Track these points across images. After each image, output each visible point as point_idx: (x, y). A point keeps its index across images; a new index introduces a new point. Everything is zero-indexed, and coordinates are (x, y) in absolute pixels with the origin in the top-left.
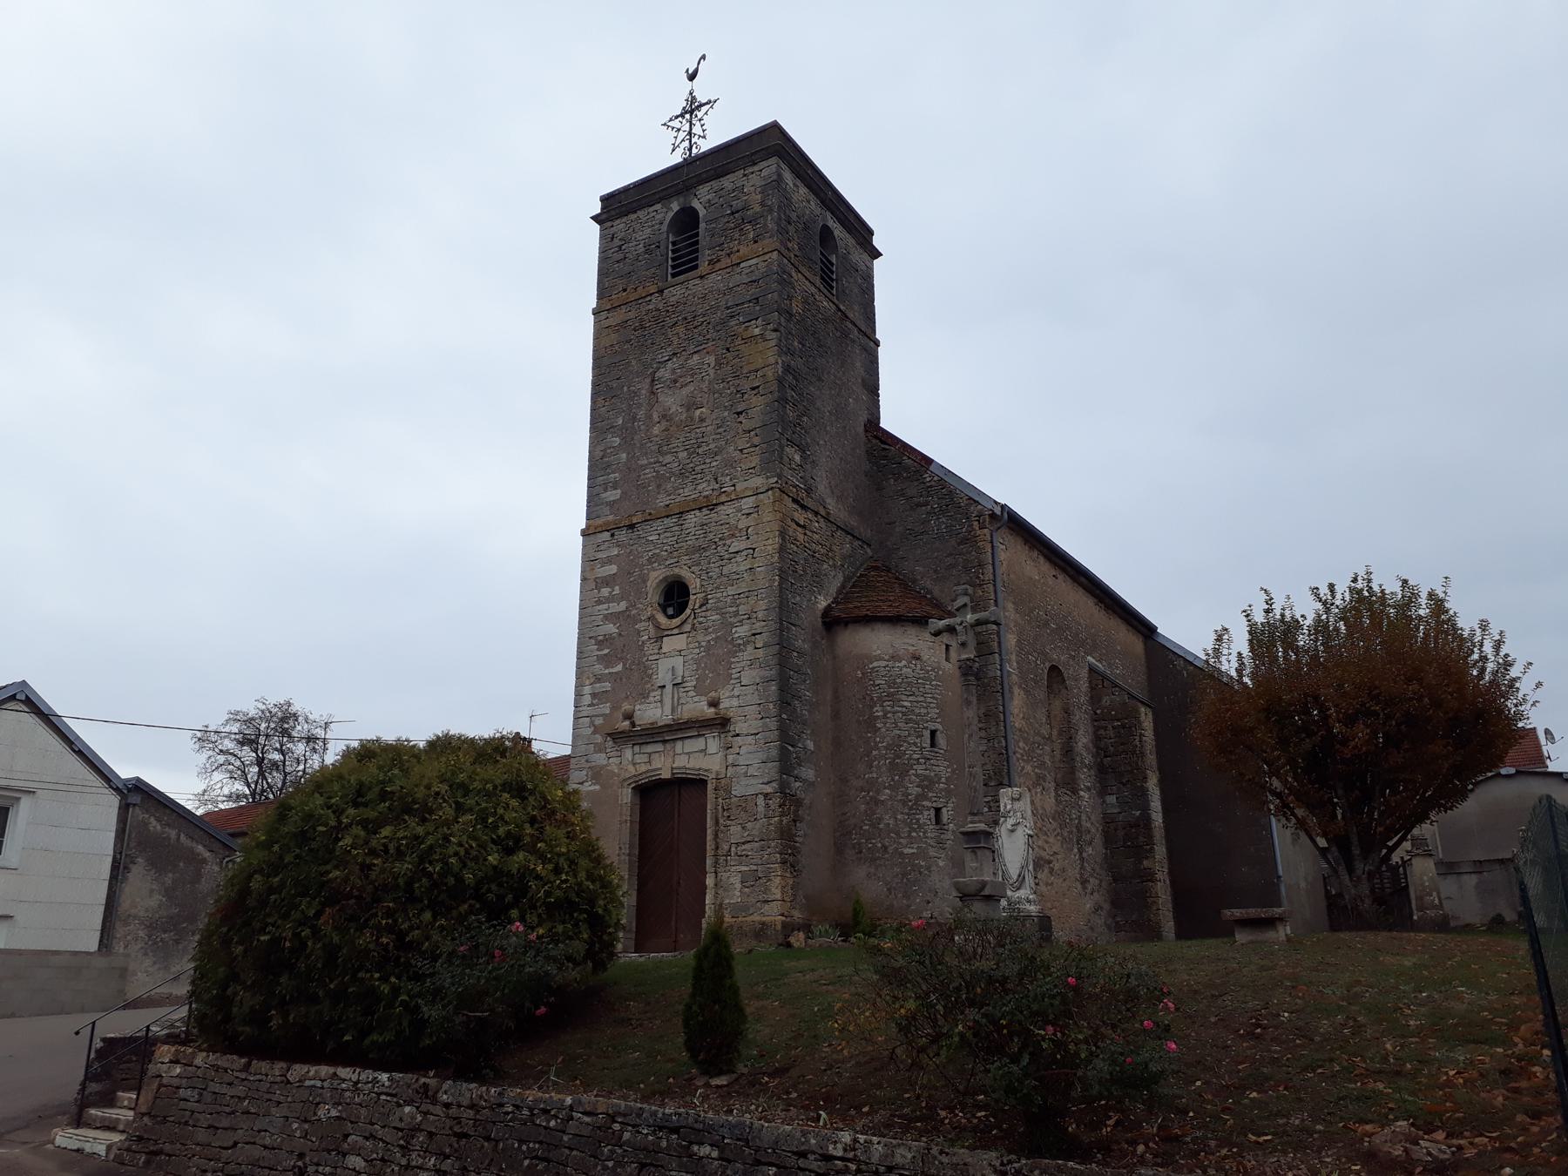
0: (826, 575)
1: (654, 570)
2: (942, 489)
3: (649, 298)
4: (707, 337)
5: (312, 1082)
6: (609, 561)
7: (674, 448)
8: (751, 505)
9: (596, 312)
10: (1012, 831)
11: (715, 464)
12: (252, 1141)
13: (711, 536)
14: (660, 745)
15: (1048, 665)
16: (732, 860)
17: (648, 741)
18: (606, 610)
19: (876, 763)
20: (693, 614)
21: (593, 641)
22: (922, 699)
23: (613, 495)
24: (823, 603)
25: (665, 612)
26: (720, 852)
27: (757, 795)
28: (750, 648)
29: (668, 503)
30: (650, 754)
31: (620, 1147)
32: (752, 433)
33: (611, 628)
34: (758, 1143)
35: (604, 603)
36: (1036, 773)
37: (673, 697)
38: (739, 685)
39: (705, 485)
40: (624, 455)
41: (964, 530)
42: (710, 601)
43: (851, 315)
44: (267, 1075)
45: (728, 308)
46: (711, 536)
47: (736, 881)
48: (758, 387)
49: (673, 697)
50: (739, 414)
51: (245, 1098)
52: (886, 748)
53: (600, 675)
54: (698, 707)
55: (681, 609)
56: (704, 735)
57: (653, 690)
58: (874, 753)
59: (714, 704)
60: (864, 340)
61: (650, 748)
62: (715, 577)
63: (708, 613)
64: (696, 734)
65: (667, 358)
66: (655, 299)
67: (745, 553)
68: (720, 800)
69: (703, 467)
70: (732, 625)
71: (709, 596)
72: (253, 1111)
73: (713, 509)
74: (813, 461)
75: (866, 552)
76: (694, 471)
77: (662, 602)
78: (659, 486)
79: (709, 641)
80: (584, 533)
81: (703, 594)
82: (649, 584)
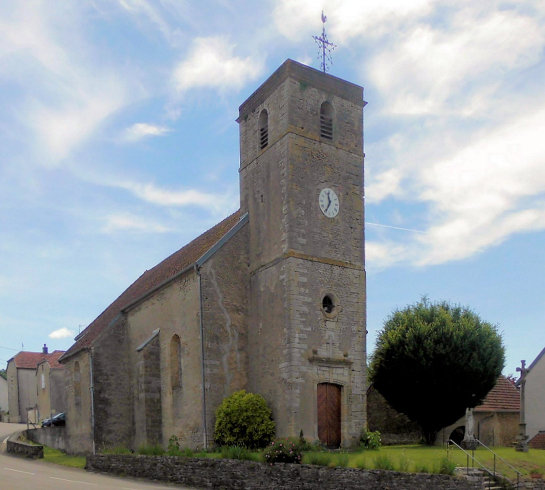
13: (343, 281)
21: (298, 313)
28: (357, 336)
33: (305, 309)
38: (353, 350)
54: (339, 355)
61: (323, 369)
71: (343, 309)
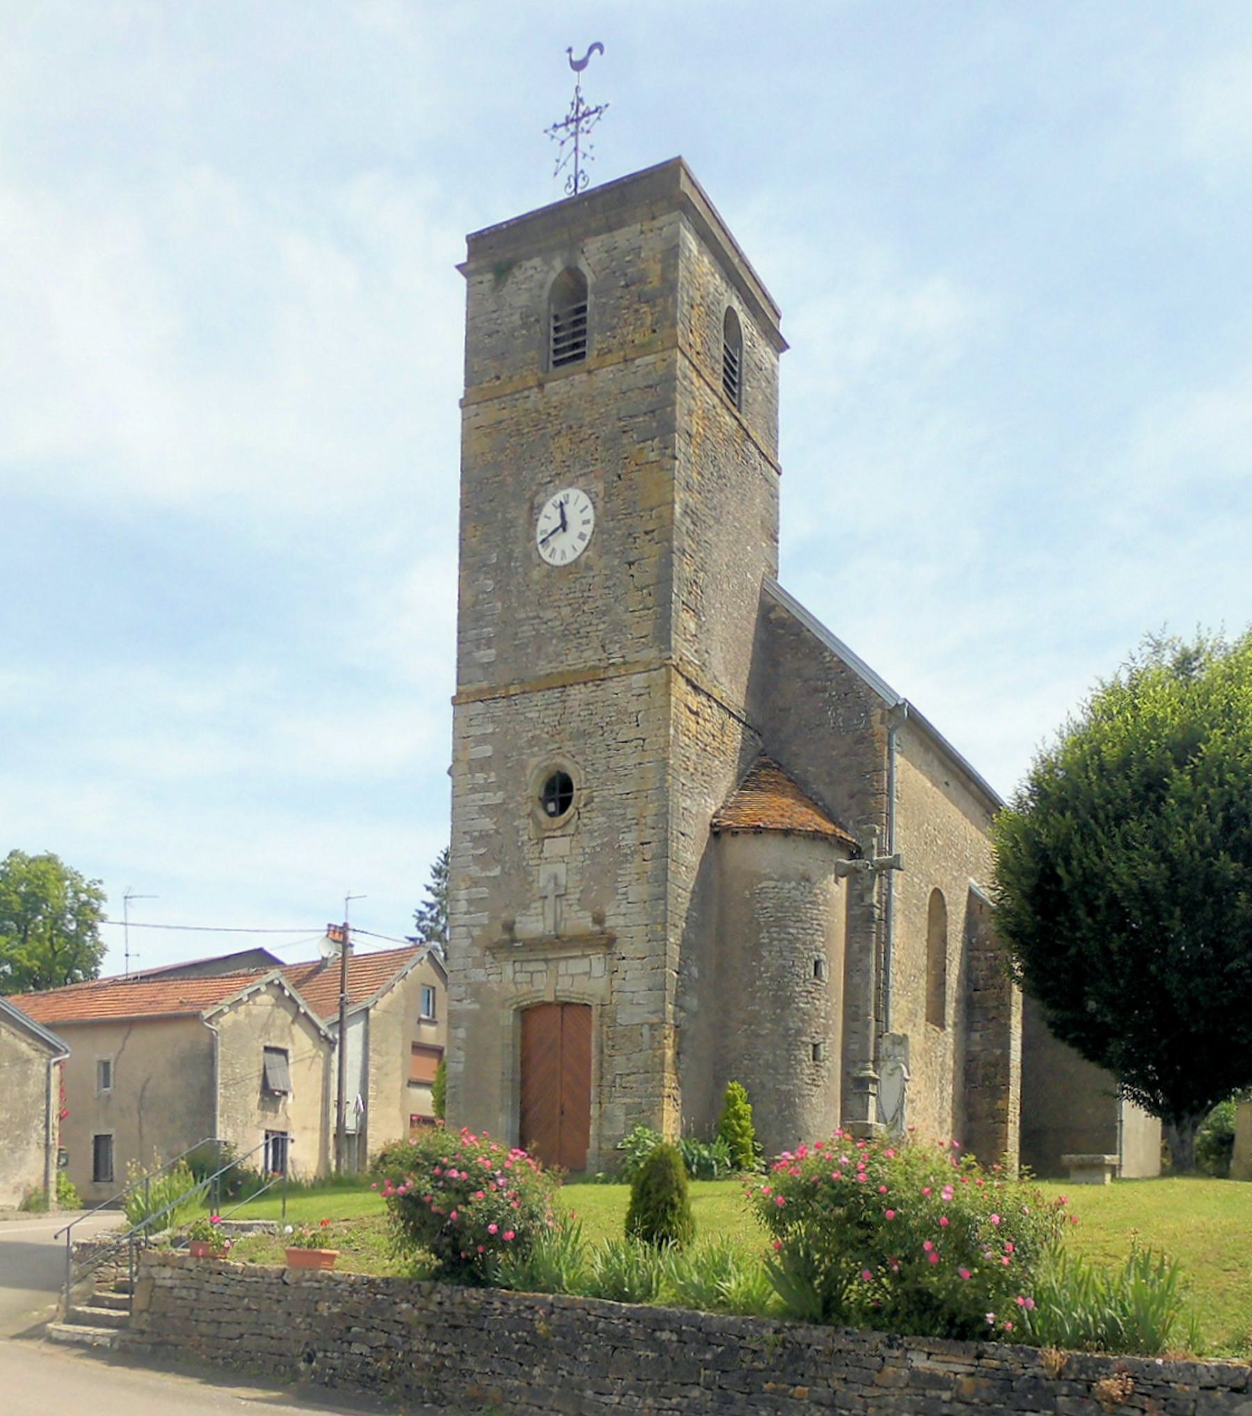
0: (716, 773)
1: (533, 755)
2: (842, 672)
3: (526, 393)
4: (596, 456)
5: (309, 1284)
6: (483, 739)
7: (556, 601)
8: (642, 684)
9: (464, 404)
10: (891, 1075)
11: (602, 626)
12: (258, 1332)
13: (597, 719)
14: (543, 963)
15: (931, 888)
16: (617, 1091)
17: (531, 958)
18: (482, 800)
19: (758, 995)
20: (576, 816)
21: (468, 838)
22: (809, 926)
23: (487, 655)
24: (712, 806)
25: (545, 809)
26: (604, 1083)
27: (642, 1025)
28: (638, 858)
29: (549, 671)
30: (532, 973)
31: (596, 1333)
32: (645, 591)
33: (487, 824)
34: (709, 1329)
35: (479, 792)
36: (909, 1009)
37: (555, 910)
38: (625, 902)
39: (590, 653)
40: (499, 605)
41: (862, 726)
42: (596, 800)
43: (752, 434)
44: (263, 1277)
45: (620, 419)
46: (597, 719)
47: (620, 1113)
48: (653, 531)
49: (555, 910)
50: (630, 564)
51: (244, 1298)
52: (771, 979)
53: (478, 878)
54: (581, 922)
55: (564, 805)
56: (589, 955)
57: (535, 901)
58: (758, 983)
59: (599, 920)
60: (766, 467)
61: (531, 967)
62: (601, 770)
63: (594, 814)
64: (580, 954)
65: (549, 479)
66: (534, 394)
67: (634, 743)
68: (605, 1028)
69: (589, 629)
70: (619, 831)
71: (595, 794)
72: (254, 1307)
73: (598, 686)
74: (708, 630)
75: (757, 745)
76: (578, 633)
77: (542, 794)
78: (539, 649)
79: (594, 847)
80: (455, 701)
81: (589, 791)
82: (528, 772)
